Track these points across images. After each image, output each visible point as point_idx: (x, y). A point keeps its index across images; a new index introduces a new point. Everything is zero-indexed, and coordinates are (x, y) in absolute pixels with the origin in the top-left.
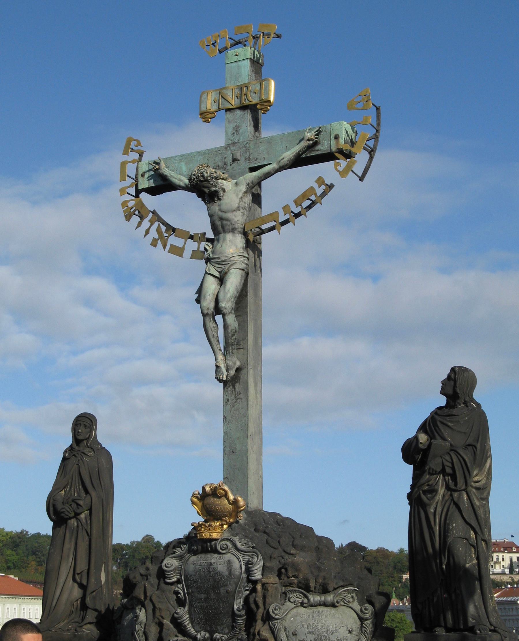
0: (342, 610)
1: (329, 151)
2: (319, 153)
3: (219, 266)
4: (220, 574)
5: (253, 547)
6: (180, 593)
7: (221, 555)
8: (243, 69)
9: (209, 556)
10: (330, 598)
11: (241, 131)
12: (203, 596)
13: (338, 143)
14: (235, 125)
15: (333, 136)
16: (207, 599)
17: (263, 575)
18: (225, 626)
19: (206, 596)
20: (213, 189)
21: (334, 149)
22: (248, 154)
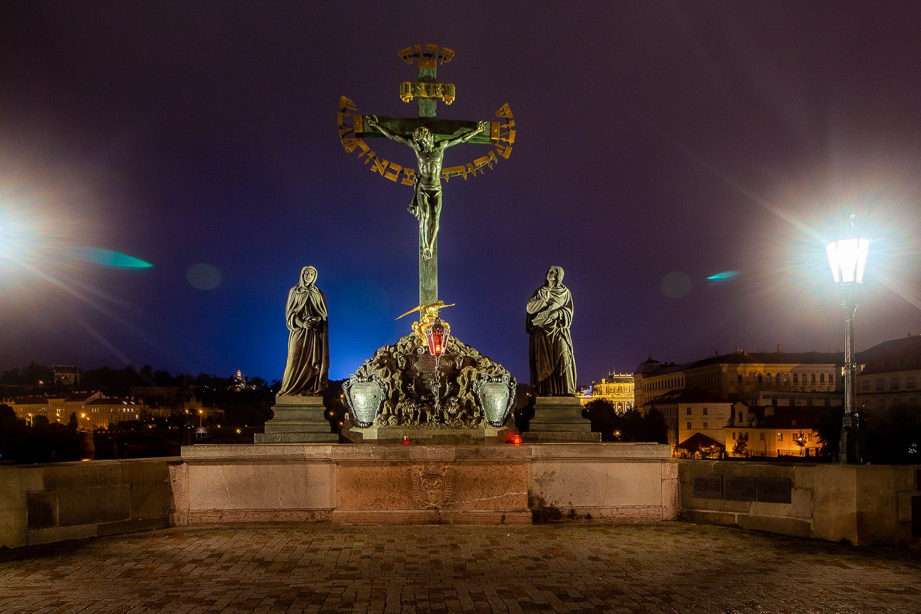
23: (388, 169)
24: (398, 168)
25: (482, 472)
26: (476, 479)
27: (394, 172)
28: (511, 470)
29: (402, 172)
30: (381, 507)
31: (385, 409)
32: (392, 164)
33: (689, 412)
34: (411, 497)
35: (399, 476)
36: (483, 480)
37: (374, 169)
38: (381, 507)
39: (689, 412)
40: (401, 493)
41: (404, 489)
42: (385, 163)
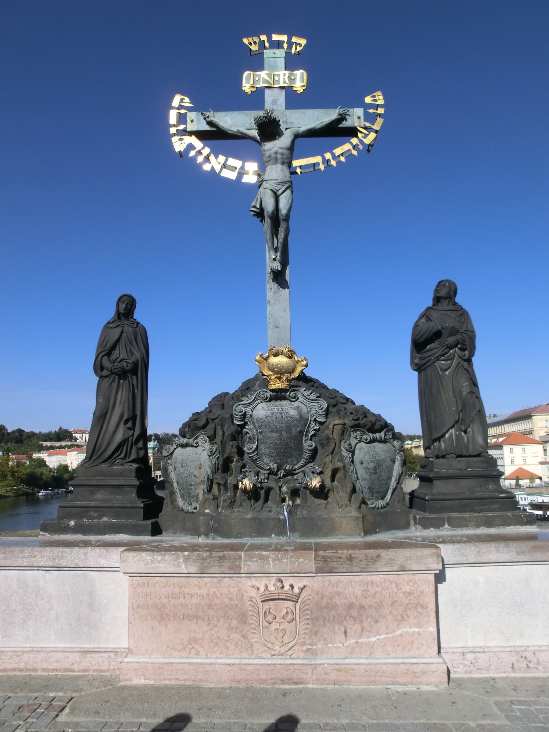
0: (388, 444)
1: (353, 126)
2: (345, 126)
3: (277, 186)
4: (292, 417)
5: (318, 397)
6: (248, 433)
7: (290, 402)
8: (279, 63)
9: (278, 402)
10: (377, 435)
11: (278, 103)
12: (275, 435)
13: (360, 122)
14: (273, 98)
15: (355, 118)
16: (278, 438)
17: (326, 418)
18: (294, 459)
19: (278, 435)
20: (275, 130)
21: (356, 125)
22: (285, 119)
23: (224, 166)
24: (237, 163)
25: (359, 593)
26: (351, 606)
27: (233, 169)
28: (407, 588)
29: (242, 168)
30: (198, 653)
31: (215, 487)
32: (230, 159)
33: (511, 451)
34: (244, 637)
35: (226, 601)
36: (362, 607)
37: (207, 167)
38: (198, 653)
39: (511, 451)
40: (230, 628)
41: (234, 623)
42: (222, 159)
